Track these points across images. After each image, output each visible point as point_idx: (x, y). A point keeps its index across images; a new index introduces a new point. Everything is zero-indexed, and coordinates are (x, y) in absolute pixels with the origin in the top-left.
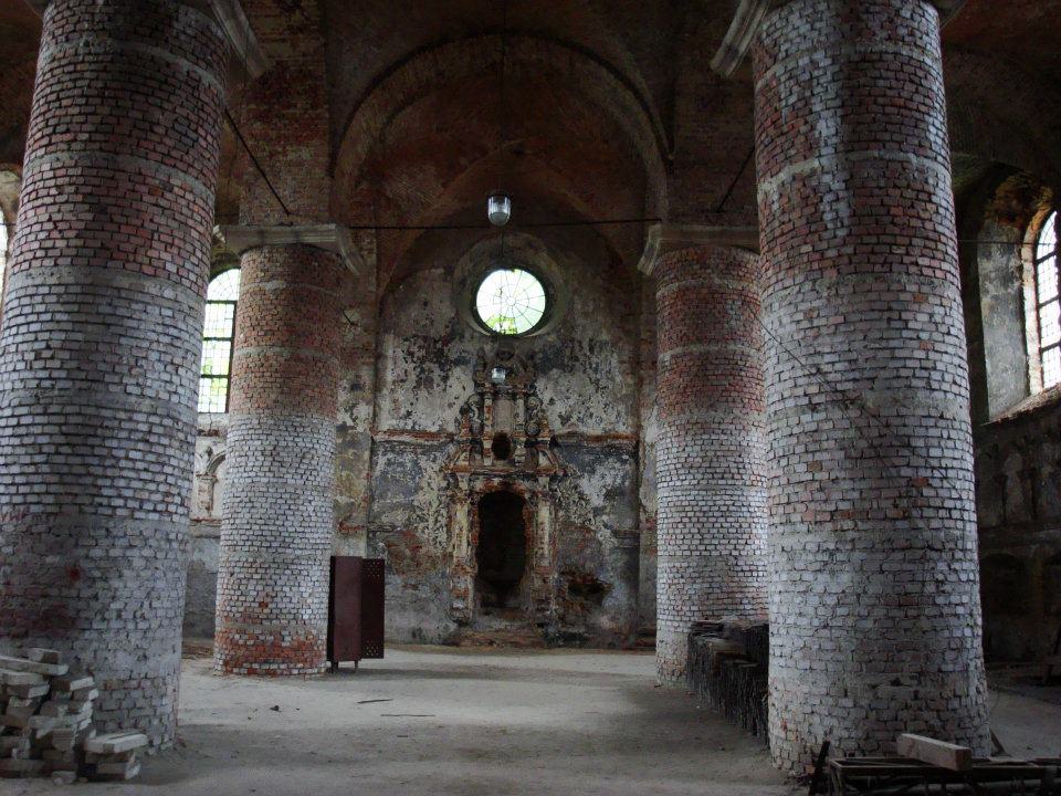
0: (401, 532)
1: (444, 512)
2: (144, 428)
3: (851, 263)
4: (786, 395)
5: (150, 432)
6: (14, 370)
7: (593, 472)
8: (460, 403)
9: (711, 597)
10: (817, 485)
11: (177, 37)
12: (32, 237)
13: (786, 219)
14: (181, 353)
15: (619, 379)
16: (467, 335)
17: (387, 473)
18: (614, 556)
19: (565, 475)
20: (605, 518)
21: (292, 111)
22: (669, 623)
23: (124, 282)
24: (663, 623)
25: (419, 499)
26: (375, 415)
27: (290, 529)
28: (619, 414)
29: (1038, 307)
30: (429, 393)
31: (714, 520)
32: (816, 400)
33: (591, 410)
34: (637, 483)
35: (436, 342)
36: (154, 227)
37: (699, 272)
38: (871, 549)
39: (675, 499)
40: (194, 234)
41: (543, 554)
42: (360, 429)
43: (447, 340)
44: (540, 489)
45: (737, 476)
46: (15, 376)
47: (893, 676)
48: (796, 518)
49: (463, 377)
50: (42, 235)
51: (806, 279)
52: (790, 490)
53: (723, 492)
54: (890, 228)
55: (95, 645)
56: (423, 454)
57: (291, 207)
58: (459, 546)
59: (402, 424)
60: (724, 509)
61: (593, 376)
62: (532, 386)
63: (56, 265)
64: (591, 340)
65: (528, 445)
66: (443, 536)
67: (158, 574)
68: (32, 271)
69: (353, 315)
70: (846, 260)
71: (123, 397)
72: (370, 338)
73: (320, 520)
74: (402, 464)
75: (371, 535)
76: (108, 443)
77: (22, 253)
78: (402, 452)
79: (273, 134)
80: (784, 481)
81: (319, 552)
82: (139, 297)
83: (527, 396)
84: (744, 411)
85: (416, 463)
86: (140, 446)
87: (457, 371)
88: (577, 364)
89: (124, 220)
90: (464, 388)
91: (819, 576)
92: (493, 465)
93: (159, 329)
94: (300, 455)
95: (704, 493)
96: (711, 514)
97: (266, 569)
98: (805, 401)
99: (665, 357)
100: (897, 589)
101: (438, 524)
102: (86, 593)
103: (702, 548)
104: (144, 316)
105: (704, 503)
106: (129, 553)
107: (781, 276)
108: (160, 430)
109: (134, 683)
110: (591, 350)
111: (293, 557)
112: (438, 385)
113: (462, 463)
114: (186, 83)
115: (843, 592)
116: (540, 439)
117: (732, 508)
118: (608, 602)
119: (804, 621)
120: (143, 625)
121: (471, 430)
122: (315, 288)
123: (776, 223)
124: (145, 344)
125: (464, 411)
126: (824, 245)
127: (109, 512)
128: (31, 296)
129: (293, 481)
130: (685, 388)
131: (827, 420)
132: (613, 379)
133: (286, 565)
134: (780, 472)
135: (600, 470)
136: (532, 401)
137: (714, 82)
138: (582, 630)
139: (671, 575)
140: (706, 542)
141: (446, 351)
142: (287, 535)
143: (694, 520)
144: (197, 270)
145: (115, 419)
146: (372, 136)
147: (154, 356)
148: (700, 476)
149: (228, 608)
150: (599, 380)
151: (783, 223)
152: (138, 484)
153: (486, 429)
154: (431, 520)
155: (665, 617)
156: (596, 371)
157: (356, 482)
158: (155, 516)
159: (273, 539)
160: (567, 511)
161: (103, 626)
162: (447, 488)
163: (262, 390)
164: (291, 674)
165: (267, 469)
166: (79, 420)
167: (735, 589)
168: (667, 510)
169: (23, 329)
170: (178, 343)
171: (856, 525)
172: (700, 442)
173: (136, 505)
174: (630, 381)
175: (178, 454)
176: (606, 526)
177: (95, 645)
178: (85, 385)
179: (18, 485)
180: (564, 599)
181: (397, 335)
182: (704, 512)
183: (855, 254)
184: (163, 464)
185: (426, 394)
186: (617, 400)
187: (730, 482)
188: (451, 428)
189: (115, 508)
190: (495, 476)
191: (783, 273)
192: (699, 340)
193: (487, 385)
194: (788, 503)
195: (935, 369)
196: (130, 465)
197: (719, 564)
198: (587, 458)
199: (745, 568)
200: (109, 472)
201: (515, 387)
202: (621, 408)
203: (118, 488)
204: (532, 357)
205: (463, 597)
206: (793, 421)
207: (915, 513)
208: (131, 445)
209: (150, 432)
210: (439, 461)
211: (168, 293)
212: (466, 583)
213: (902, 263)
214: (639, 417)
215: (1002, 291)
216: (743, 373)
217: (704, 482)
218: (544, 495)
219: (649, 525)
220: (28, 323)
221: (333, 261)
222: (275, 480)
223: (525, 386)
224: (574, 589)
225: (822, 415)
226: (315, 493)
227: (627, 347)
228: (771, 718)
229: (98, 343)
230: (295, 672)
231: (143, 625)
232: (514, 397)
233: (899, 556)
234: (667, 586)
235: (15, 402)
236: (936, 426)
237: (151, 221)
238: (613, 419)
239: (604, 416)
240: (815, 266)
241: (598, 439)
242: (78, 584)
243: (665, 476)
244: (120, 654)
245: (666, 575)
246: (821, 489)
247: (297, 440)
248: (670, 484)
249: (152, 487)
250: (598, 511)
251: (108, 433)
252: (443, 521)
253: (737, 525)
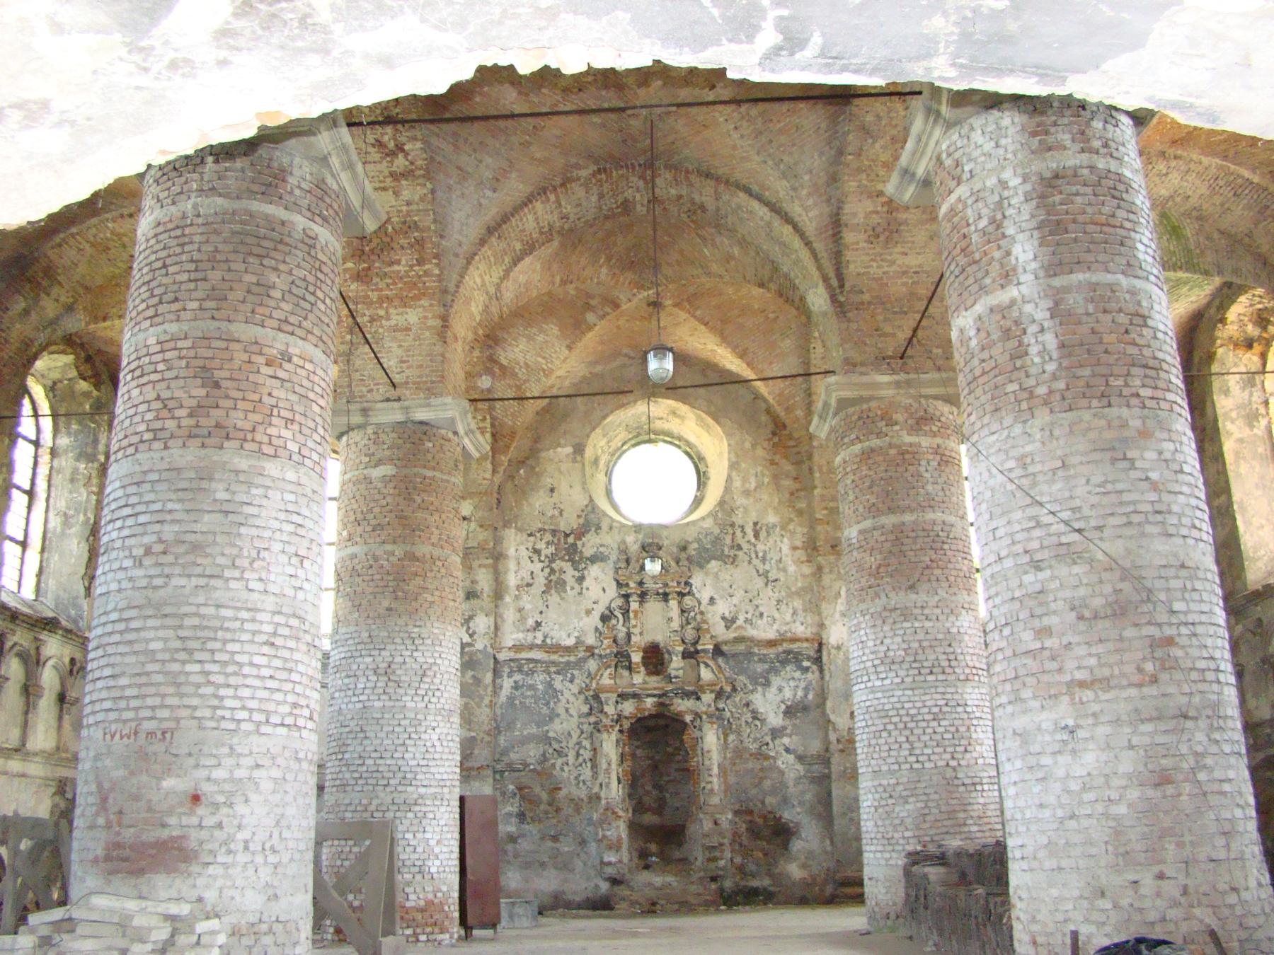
0: (534, 771)
1: (586, 743)
2: (269, 628)
3: (1064, 399)
4: (1003, 554)
5: (275, 634)
6: (121, 568)
7: (767, 684)
8: (600, 609)
9: (928, 818)
10: (1047, 653)
11: (291, 193)
12: (138, 419)
13: (985, 355)
14: (306, 543)
15: (792, 568)
16: (604, 525)
17: (515, 698)
18: (801, 787)
19: (734, 689)
20: (786, 740)
21: (396, 268)
22: (879, 855)
23: (242, 463)
24: (871, 855)
25: (556, 728)
26: (497, 628)
27: (411, 763)
28: (794, 613)
30: (562, 599)
31: (924, 724)
32: (1038, 557)
33: (761, 609)
34: (822, 696)
35: (567, 535)
36: (273, 401)
37: (884, 429)
38: (1117, 722)
39: (876, 702)
40: (316, 408)
41: (712, 790)
42: (479, 646)
43: (581, 533)
44: (704, 709)
45: (948, 670)
46: (121, 575)
47: (1156, 869)
48: (1026, 694)
49: (602, 576)
50: (149, 416)
51: (1015, 421)
52: (1017, 662)
53: (933, 690)
54: (1104, 357)
55: (220, 883)
56: (558, 673)
57: (397, 379)
58: (608, 785)
59: (530, 637)
60: (936, 710)
61: (761, 568)
62: (687, 583)
63: (166, 448)
64: (755, 524)
65: (686, 655)
66: (587, 773)
67: (289, 798)
68: (138, 456)
69: (466, 508)
70: (1058, 397)
71: (244, 595)
72: (482, 535)
73: (447, 750)
74: (532, 687)
75: (498, 777)
76: (230, 647)
77: (126, 437)
78: (532, 672)
79: (374, 296)
80: (1008, 653)
81: (446, 790)
82: (258, 480)
83: (681, 595)
84: (952, 591)
85: (549, 685)
86: (266, 649)
87: (594, 571)
88: (740, 553)
89: (239, 395)
90: (604, 590)
91: (1060, 759)
92: (645, 682)
93: (282, 516)
94: (420, 672)
95: (910, 693)
96: (920, 717)
97: (384, 812)
98: (1026, 559)
99: (851, 533)
100: (1150, 766)
101: (581, 759)
102: (210, 821)
103: (913, 759)
104: (265, 502)
105: (910, 705)
106: (256, 773)
107: (986, 420)
108: (286, 631)
109: (264, 927)
110: (756, 536)
111: (415, 796)
112: (572, 588)
113: (606, 681)
114: (303, 242)
115: (1089, 774)
116: (700, 648)
117: (945, 709)
118: (797, 845)
119: (1047, 813)
120: (272, 859)
121: (615, 641)
122: (429, 473)
123: (976, 361)
124: (267, 534)
125: (604, 619)
126: (1032, 382)
127: (232, 726)
128: (138, 484)
129: (413, 704)
130: (879, 566)
131: (1053, 578)
132: (785, 570)
133: (409, 806)
134: (1003, 644)
135: (776, 681)
136: (688, 601)
137: (885, 209)
138: (766, 882)
139: (877, 796)
140: (917, 752)
141: (579, 546)
142: (407, 769)
143: (901, 726)
144: (319, 449)
145: (237, 619)
146: (487, 293)
147: (277, 547)
148: (902, 673)
149: (339, 863)
150: (768, 572)
151: (983, 361)
152: (265, 694)
153: (634, 639)
154: (572, 754)
155: (873, 848)
156: (764, 560)
157: (478, 711)
158: (283, 731)
159: (391, 775)
160: (739, 734)
161: (229, 859)
162: (590, 714)
163: (371, 597)
164: (418, 940)
165: (381, 691)
166: (196, 621)
167: (958, 808)
168: (867, 716)
169: (130, 522)
170: (301, 531)
171: (1097, 696)
172: (901, 632)
173: (262, 718)
174: (807, 570)
175: (306, 659)
176: (787, 750)
177: (220, 883)
178: (202, 581)
179: (128, 698)
180: (741, 845)
181: (519, 530)
182: (912, 716)
183: (1068, 389)
184: (291, 671)
185: (558, 599)
186: (791, 595)
187: (941, 677)
188: (591, 640)
189: (239, 721)
190: (648, 696)
191: (988, 416)
192: (891, 510)
193: (632, 585)
194: (1016, 678)
195: (1170, 512)
196: (254, 671)
197: (935, 778)
198: (760, 668)
199: (967, 781)
200: (232, 680)
201: (666, 585)
202: (798, 603)
203: (241, 698)
204: (684, 549)
205: (615, 846)
206: (1014, 583)
207: (1164, 677)
208: (254, 649)
209: (275, 634)
210: (576, 681)
211: (291, 475)
212: (619, 830)
213: (1120, 395)
214: (820, 614)
216: (946, 546)
217: (909, 680)
218: (710, 716)
219: (841, 746)
220: (136, 515)
221: (449, 440)
222: (391, 704)
223: (679, 583)
224: (754, 833)
225: (1048, 573)
226: (439, 718)
227: (799, 529)
228: (1016, 935)
229: (215, 533)
230: (423, 938)
231: (272, 859)
232: (665, 597)
233: (1148, 727)
234: (873, 809)
235: (122, 604)
236: (1177, 577)
237: (270, 394)
238: (788, 618)
239: (777, 615)
240: (1024, 405)
241: (771, 643)
242: (201, 811)
243: (862, 676)
244: (250, 893)
245: (870, 796)
246: (1053, 658)
247: (415, 654)
248: (869, 684)
249: (279, 696)
250: (776, 733)
251: (229, 636)
252: (587, 754)
253: (953, 729)
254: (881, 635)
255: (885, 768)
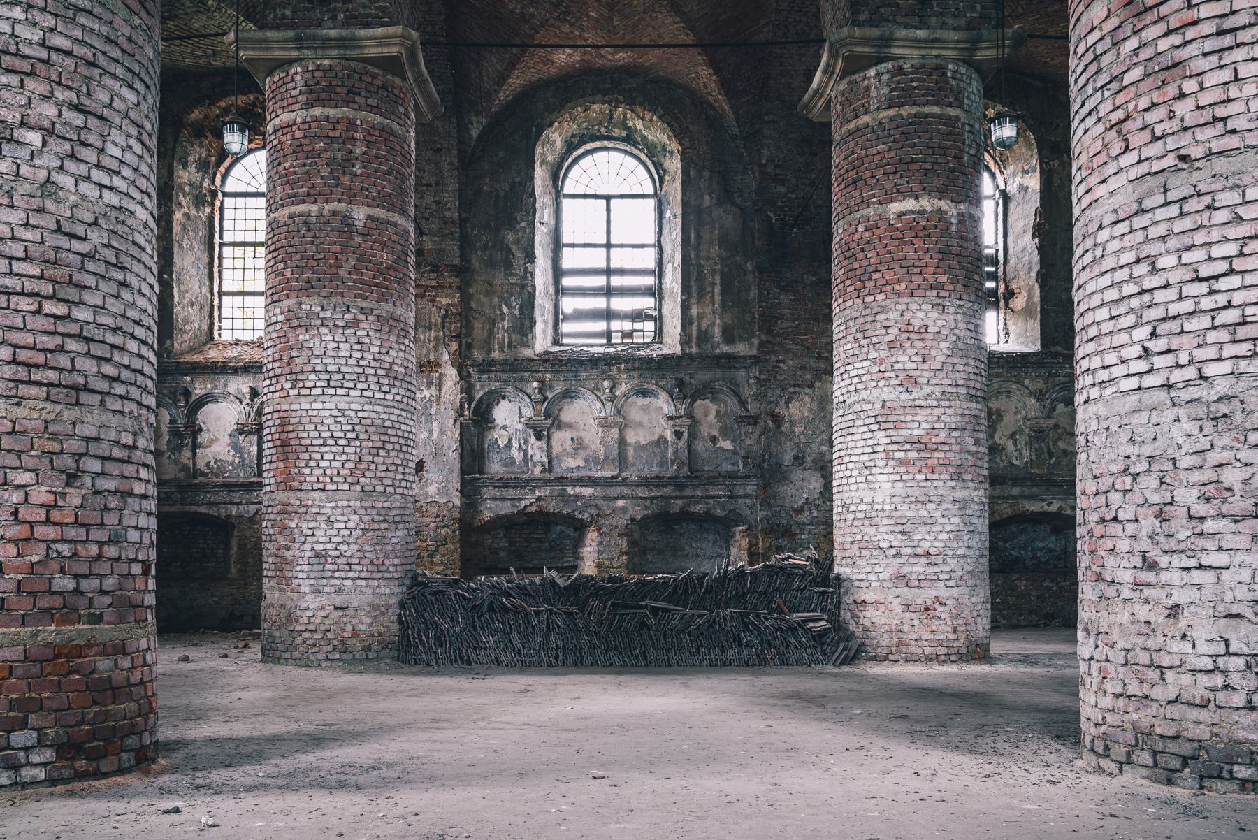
29: (221, 245)
39: (373, 415)
215: (193, 212)
245: (356, 517)
254: (387, 344)
255: (380, 489)
